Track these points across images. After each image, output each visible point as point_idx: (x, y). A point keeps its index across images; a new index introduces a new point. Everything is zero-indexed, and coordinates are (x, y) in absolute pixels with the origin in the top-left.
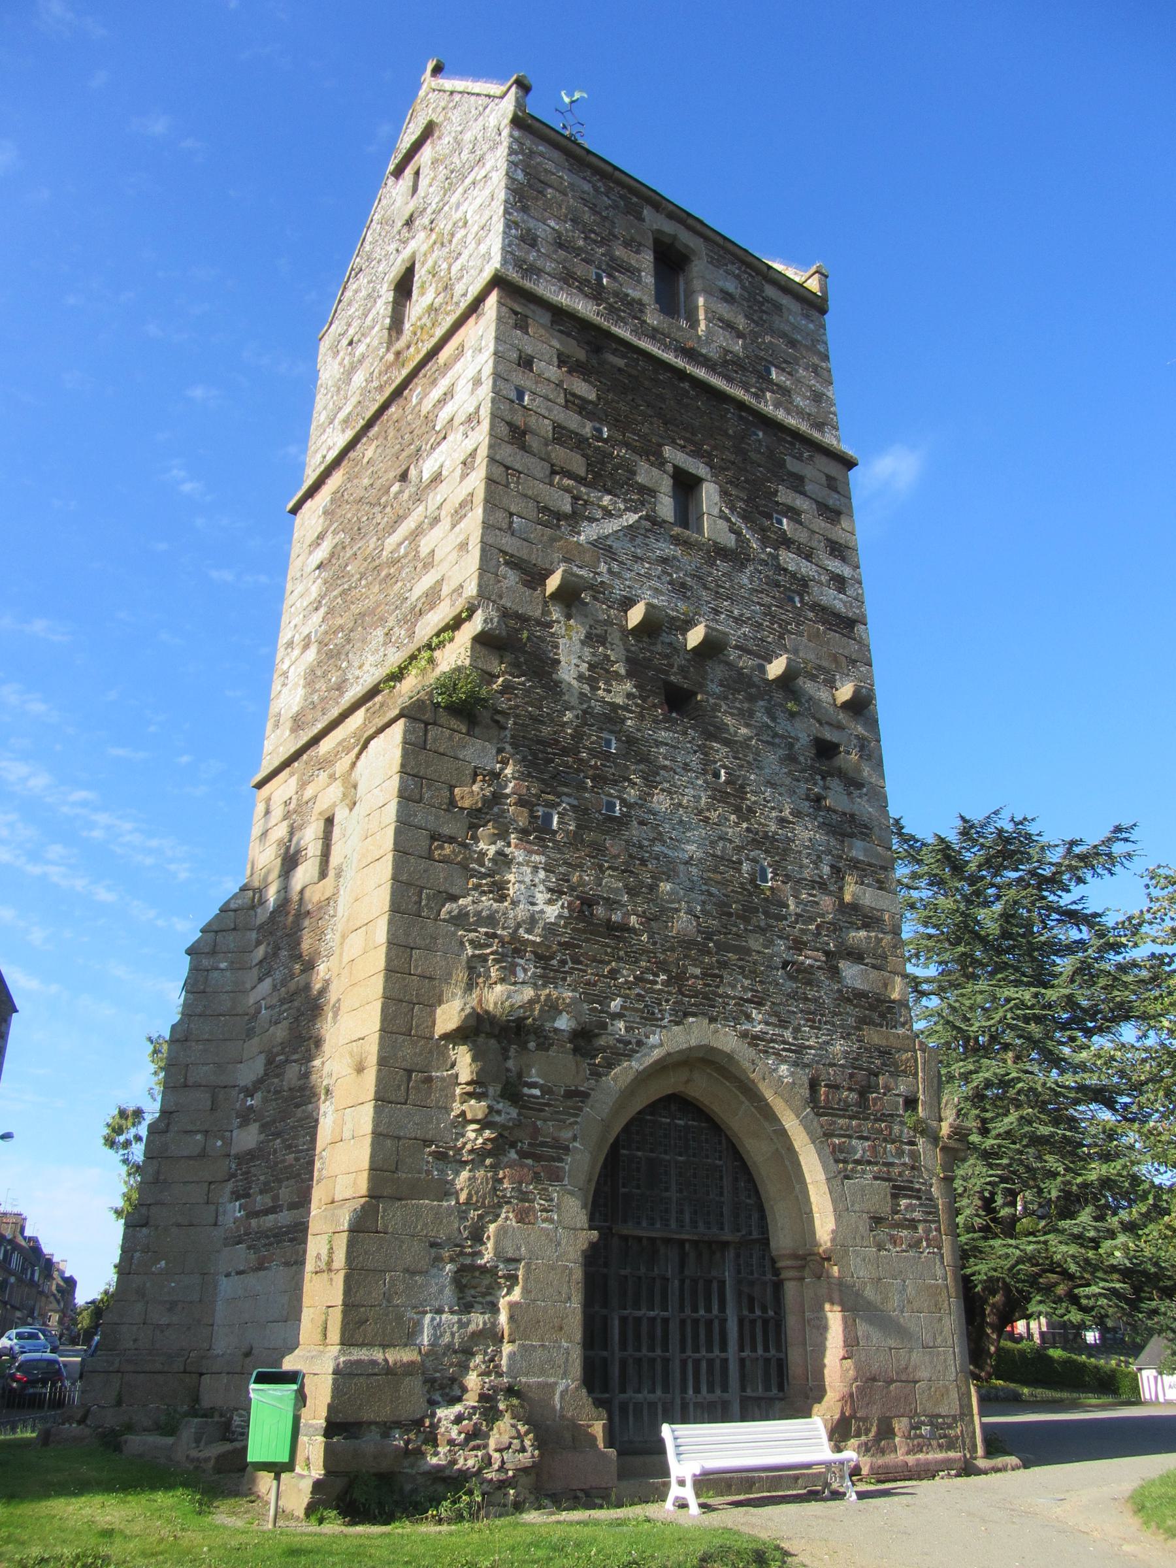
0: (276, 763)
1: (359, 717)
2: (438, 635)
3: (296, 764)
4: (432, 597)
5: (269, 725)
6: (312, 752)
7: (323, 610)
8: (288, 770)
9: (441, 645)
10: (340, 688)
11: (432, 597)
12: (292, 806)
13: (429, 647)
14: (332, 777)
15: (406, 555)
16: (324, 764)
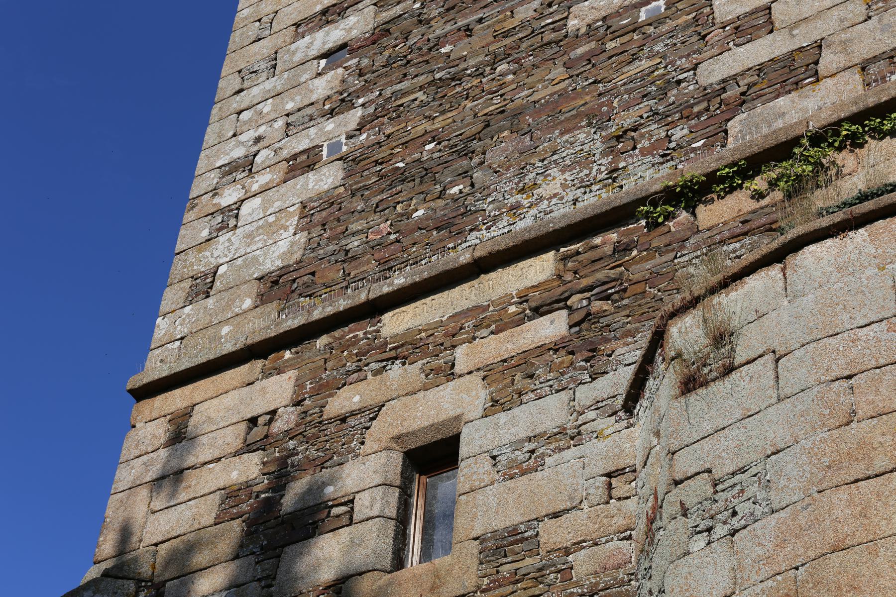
0: (229, 347)
1: (539, 269)
2: (857, 118)
3: (288, 355)
4: (796, 70)
5: (171, 296)
6: (358, 332)
7: (354, 116)
8: (259, 364)
9: (855, 142)
10: (451, 226)
11: (796, 70)
12: (278, 426)
13: (817, 139)
14: (449, 373)
15: (657, 21)
16: (406, 350)
